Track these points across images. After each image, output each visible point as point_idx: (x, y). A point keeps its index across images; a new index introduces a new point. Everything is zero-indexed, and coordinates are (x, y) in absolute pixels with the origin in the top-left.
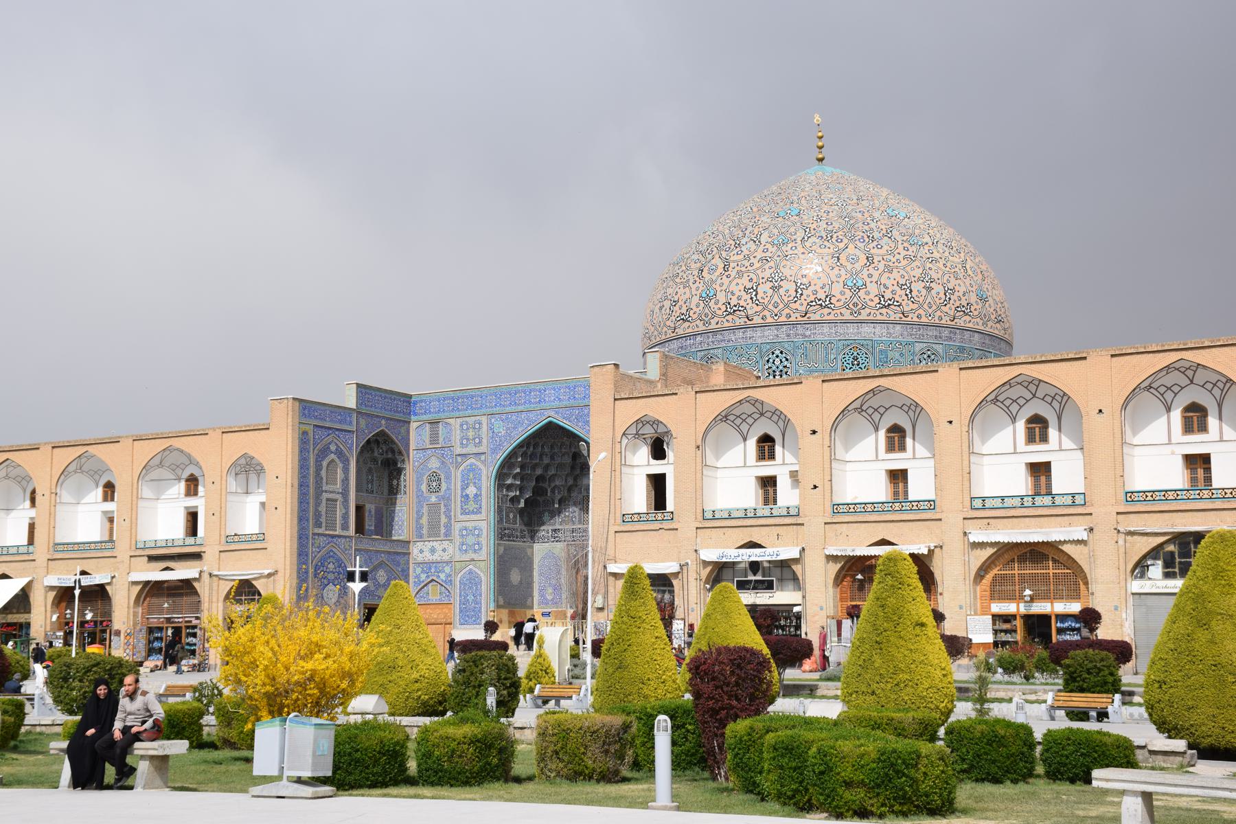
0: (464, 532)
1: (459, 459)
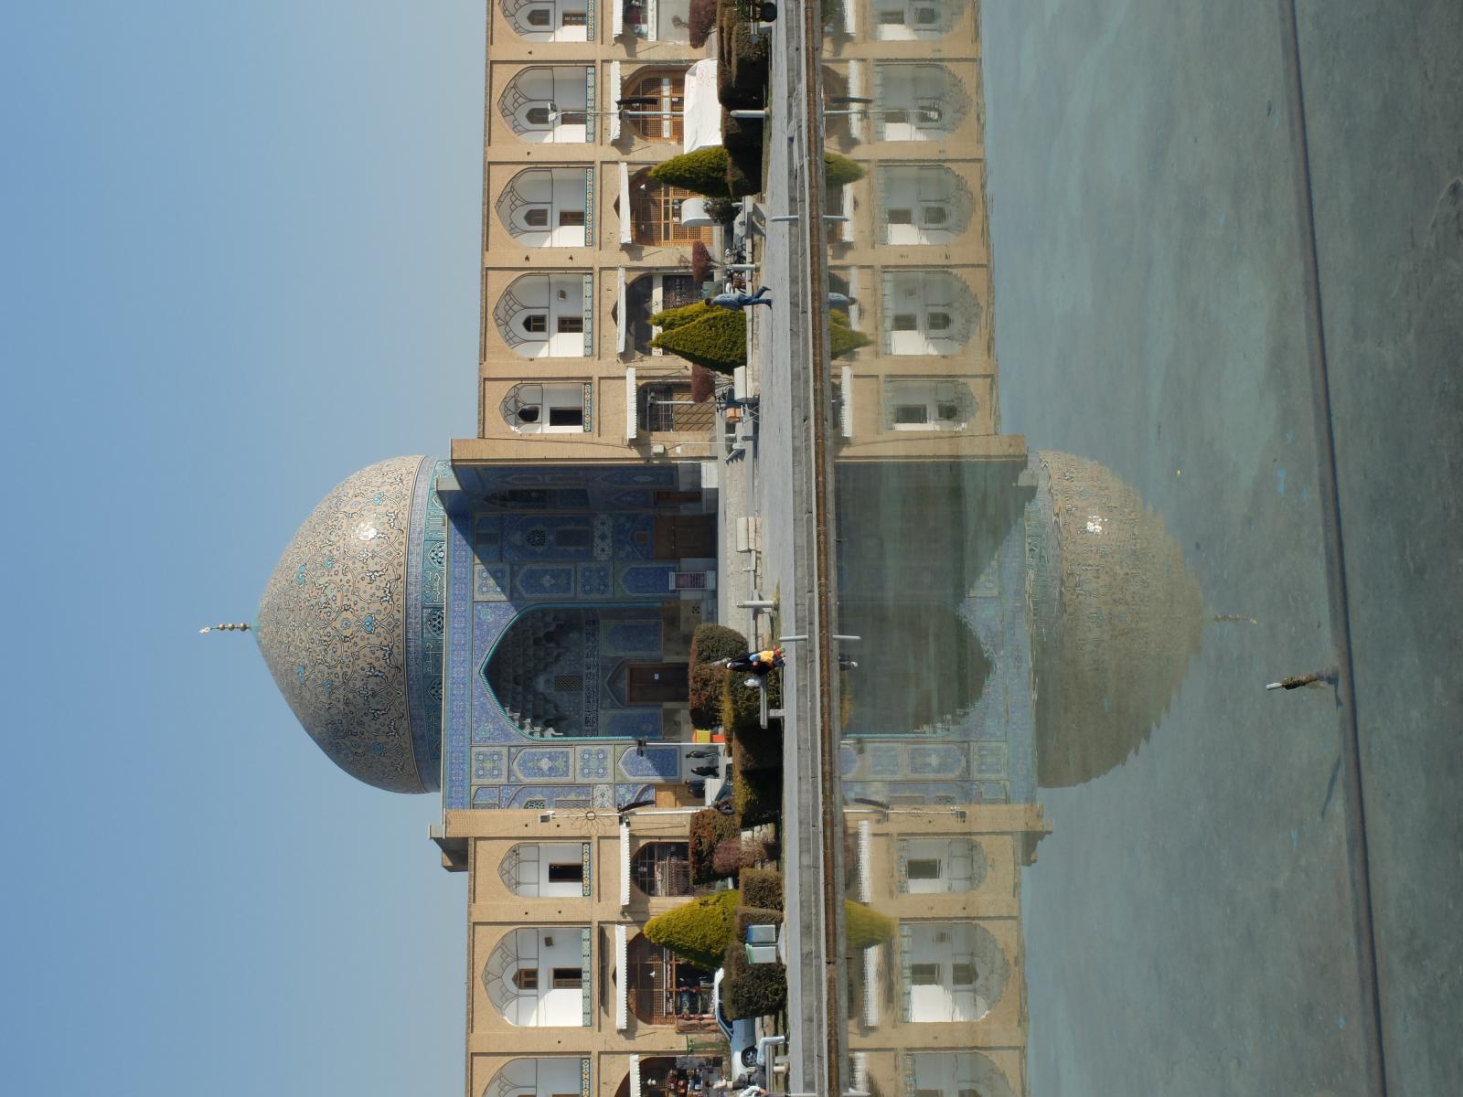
0: (586, 771)
1: (512, 779)
